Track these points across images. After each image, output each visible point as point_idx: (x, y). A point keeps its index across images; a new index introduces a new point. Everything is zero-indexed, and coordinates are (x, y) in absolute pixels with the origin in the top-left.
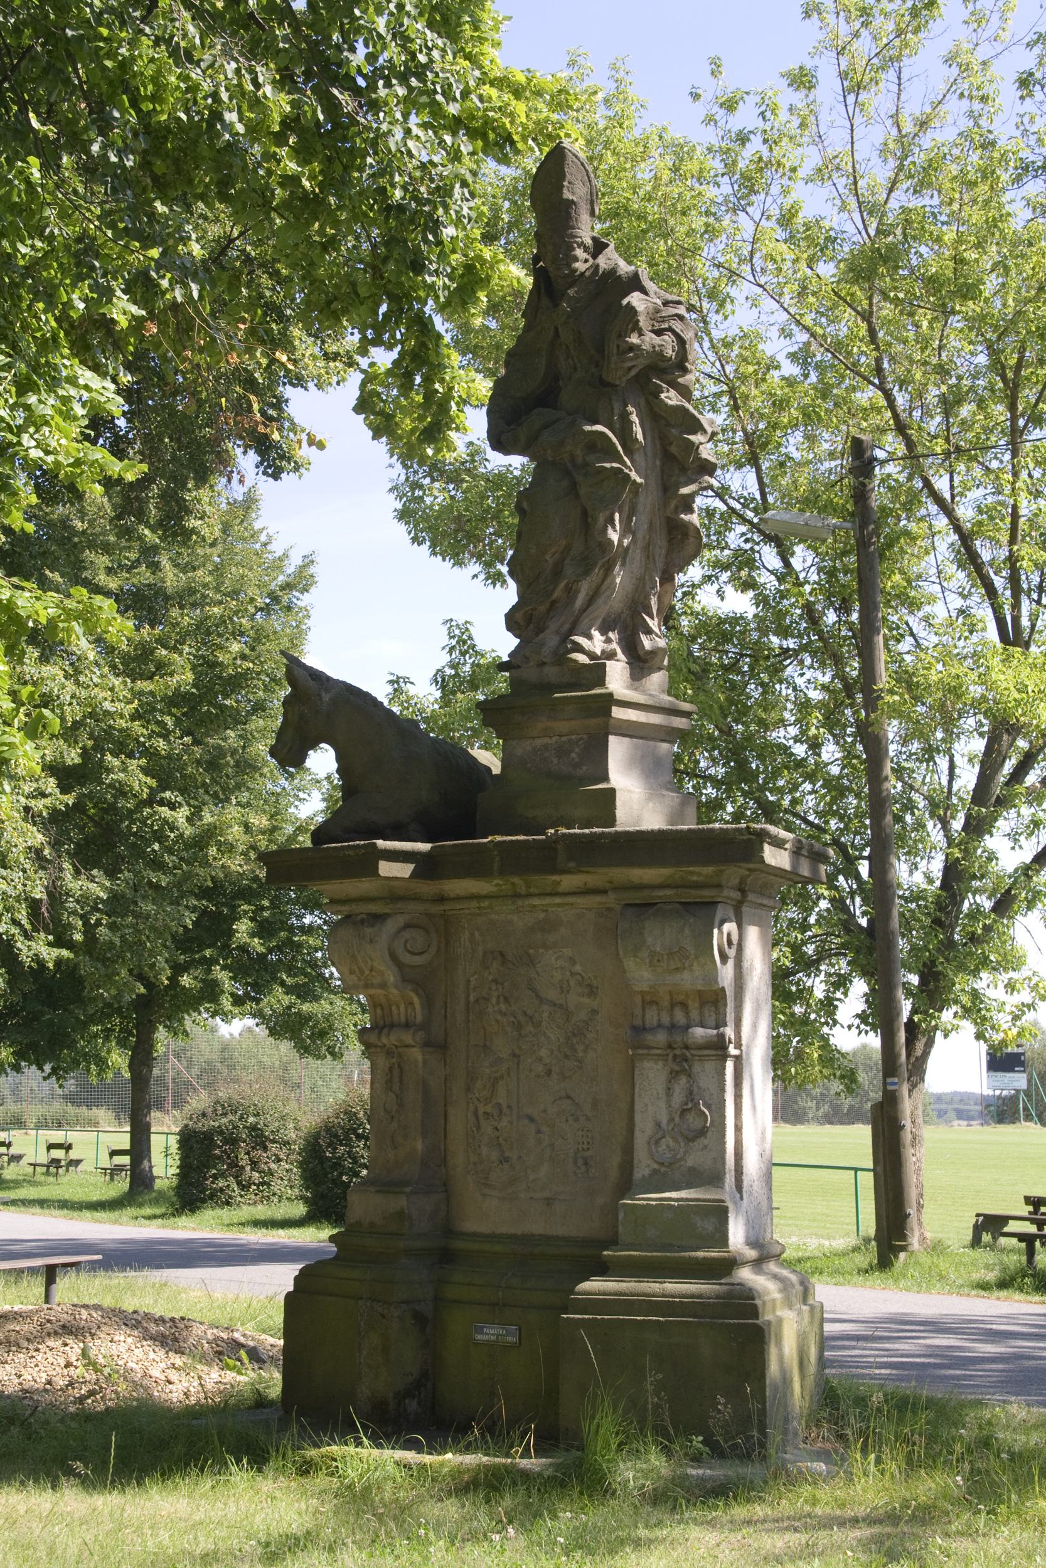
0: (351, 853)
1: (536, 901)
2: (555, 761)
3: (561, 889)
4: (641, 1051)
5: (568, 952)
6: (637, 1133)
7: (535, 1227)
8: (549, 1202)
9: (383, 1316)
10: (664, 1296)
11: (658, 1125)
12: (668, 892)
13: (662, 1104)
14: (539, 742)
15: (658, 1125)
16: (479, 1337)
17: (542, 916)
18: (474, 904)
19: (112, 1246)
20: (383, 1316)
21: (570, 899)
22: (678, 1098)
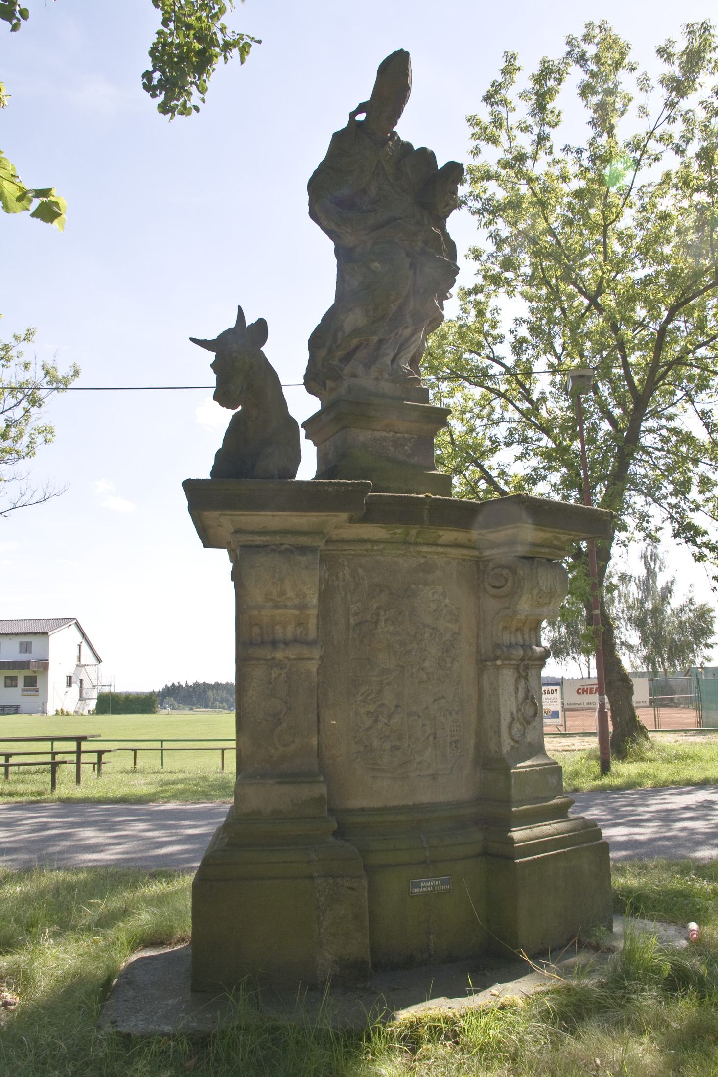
0: (330, 489)
1: (424, 549)
2: (392, 450)
3: (439, 542)
4: (506, 662)
5: (439, 588)
6: (502, 721)
7: (425, 797)
8: (434, 777)
9: (353, 889)
10: (559, 834)
11: (512, 714)
12: (546, 550)
13: (513, 699)
14: (378, 434)
15: (512, 714)
16: (417, 890)
17: (422, 560)
18: (369, 546)
19: (704, 848)
20: (353, 889)
21: (449, 550)
22: (521, 695)
